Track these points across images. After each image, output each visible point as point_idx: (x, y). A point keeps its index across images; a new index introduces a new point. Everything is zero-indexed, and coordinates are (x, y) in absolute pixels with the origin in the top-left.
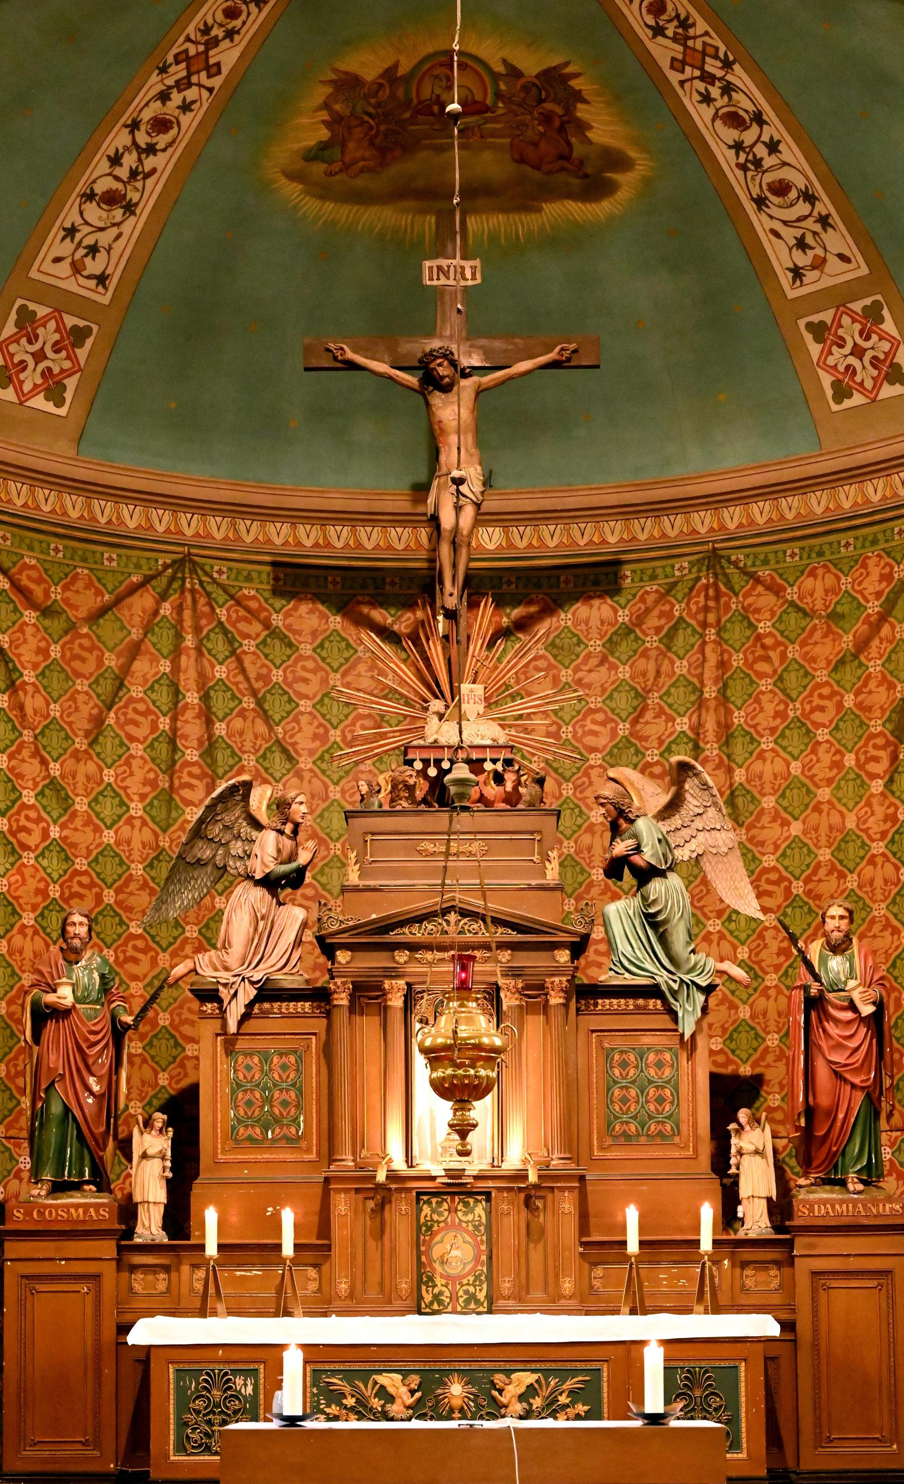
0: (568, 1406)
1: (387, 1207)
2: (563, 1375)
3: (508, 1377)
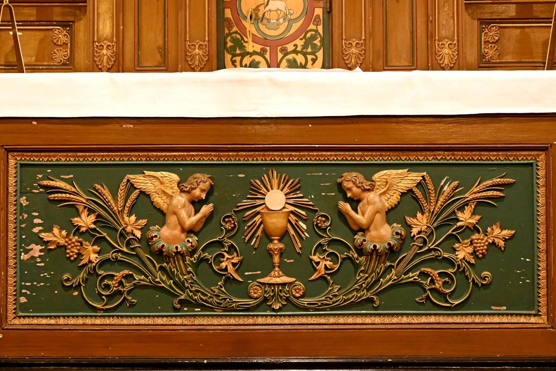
0: (475, 229)
2: (467, 172)
3: (369, 178)
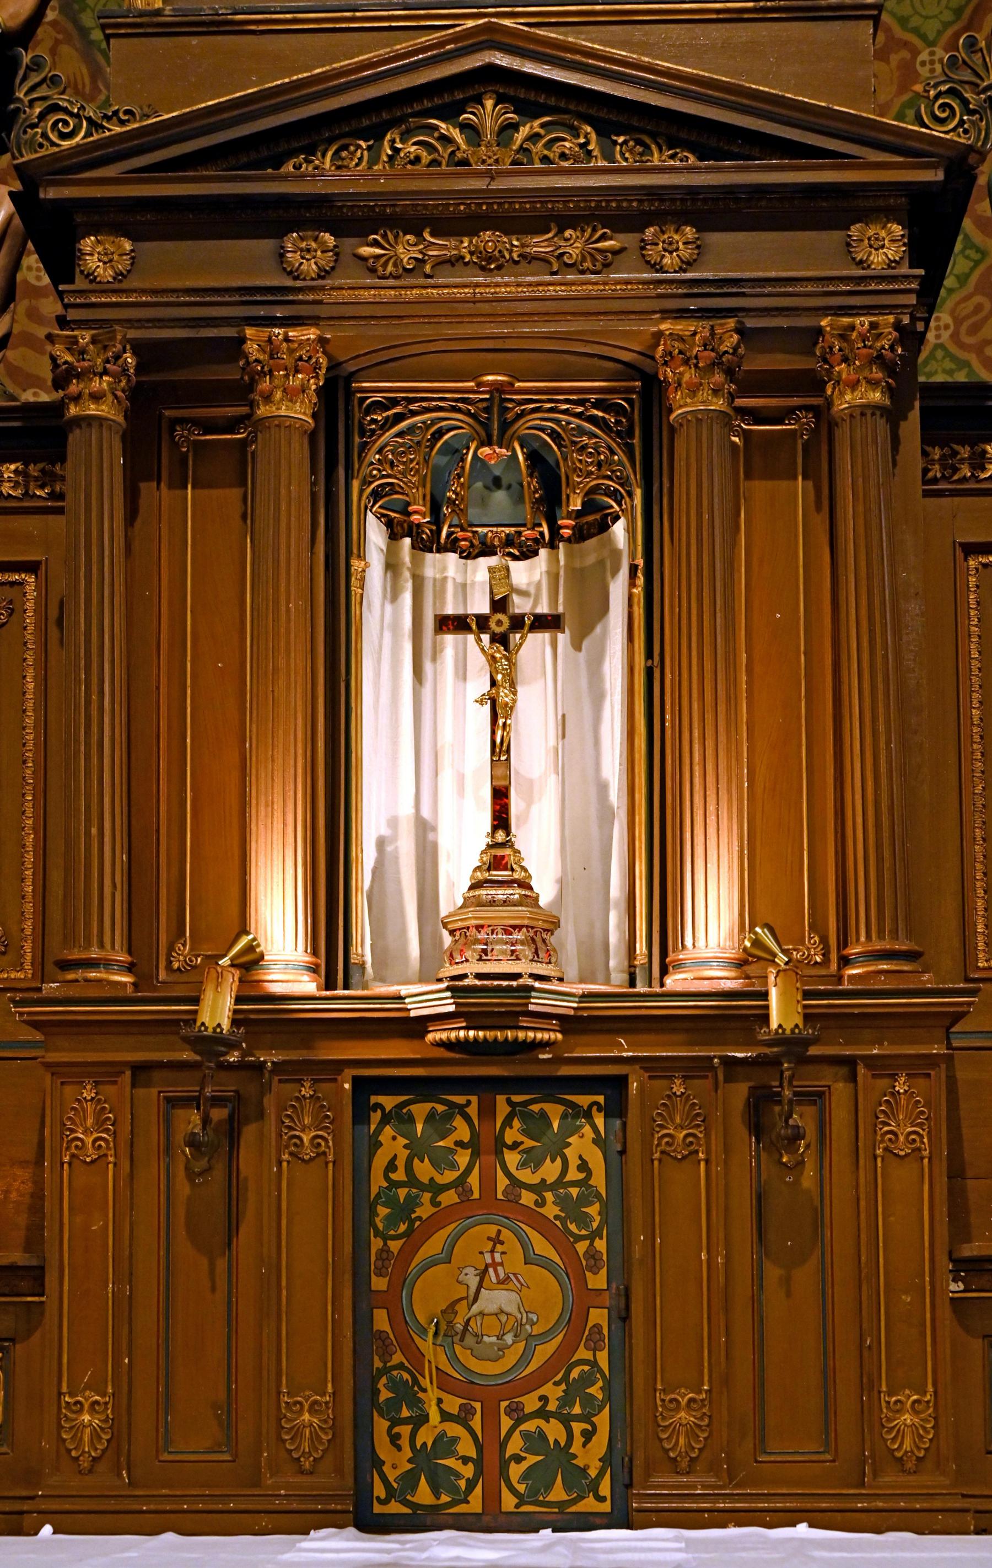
1: (249, 1132)
